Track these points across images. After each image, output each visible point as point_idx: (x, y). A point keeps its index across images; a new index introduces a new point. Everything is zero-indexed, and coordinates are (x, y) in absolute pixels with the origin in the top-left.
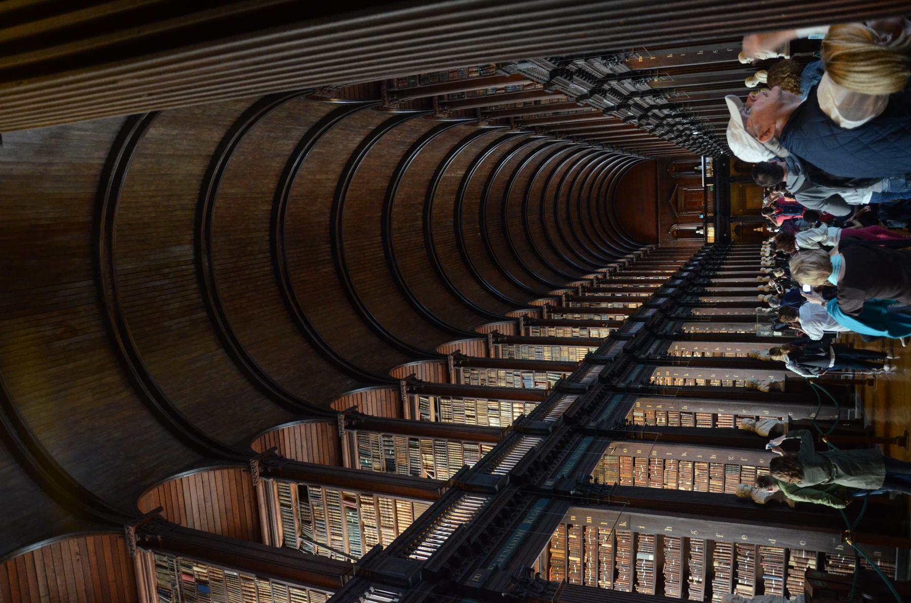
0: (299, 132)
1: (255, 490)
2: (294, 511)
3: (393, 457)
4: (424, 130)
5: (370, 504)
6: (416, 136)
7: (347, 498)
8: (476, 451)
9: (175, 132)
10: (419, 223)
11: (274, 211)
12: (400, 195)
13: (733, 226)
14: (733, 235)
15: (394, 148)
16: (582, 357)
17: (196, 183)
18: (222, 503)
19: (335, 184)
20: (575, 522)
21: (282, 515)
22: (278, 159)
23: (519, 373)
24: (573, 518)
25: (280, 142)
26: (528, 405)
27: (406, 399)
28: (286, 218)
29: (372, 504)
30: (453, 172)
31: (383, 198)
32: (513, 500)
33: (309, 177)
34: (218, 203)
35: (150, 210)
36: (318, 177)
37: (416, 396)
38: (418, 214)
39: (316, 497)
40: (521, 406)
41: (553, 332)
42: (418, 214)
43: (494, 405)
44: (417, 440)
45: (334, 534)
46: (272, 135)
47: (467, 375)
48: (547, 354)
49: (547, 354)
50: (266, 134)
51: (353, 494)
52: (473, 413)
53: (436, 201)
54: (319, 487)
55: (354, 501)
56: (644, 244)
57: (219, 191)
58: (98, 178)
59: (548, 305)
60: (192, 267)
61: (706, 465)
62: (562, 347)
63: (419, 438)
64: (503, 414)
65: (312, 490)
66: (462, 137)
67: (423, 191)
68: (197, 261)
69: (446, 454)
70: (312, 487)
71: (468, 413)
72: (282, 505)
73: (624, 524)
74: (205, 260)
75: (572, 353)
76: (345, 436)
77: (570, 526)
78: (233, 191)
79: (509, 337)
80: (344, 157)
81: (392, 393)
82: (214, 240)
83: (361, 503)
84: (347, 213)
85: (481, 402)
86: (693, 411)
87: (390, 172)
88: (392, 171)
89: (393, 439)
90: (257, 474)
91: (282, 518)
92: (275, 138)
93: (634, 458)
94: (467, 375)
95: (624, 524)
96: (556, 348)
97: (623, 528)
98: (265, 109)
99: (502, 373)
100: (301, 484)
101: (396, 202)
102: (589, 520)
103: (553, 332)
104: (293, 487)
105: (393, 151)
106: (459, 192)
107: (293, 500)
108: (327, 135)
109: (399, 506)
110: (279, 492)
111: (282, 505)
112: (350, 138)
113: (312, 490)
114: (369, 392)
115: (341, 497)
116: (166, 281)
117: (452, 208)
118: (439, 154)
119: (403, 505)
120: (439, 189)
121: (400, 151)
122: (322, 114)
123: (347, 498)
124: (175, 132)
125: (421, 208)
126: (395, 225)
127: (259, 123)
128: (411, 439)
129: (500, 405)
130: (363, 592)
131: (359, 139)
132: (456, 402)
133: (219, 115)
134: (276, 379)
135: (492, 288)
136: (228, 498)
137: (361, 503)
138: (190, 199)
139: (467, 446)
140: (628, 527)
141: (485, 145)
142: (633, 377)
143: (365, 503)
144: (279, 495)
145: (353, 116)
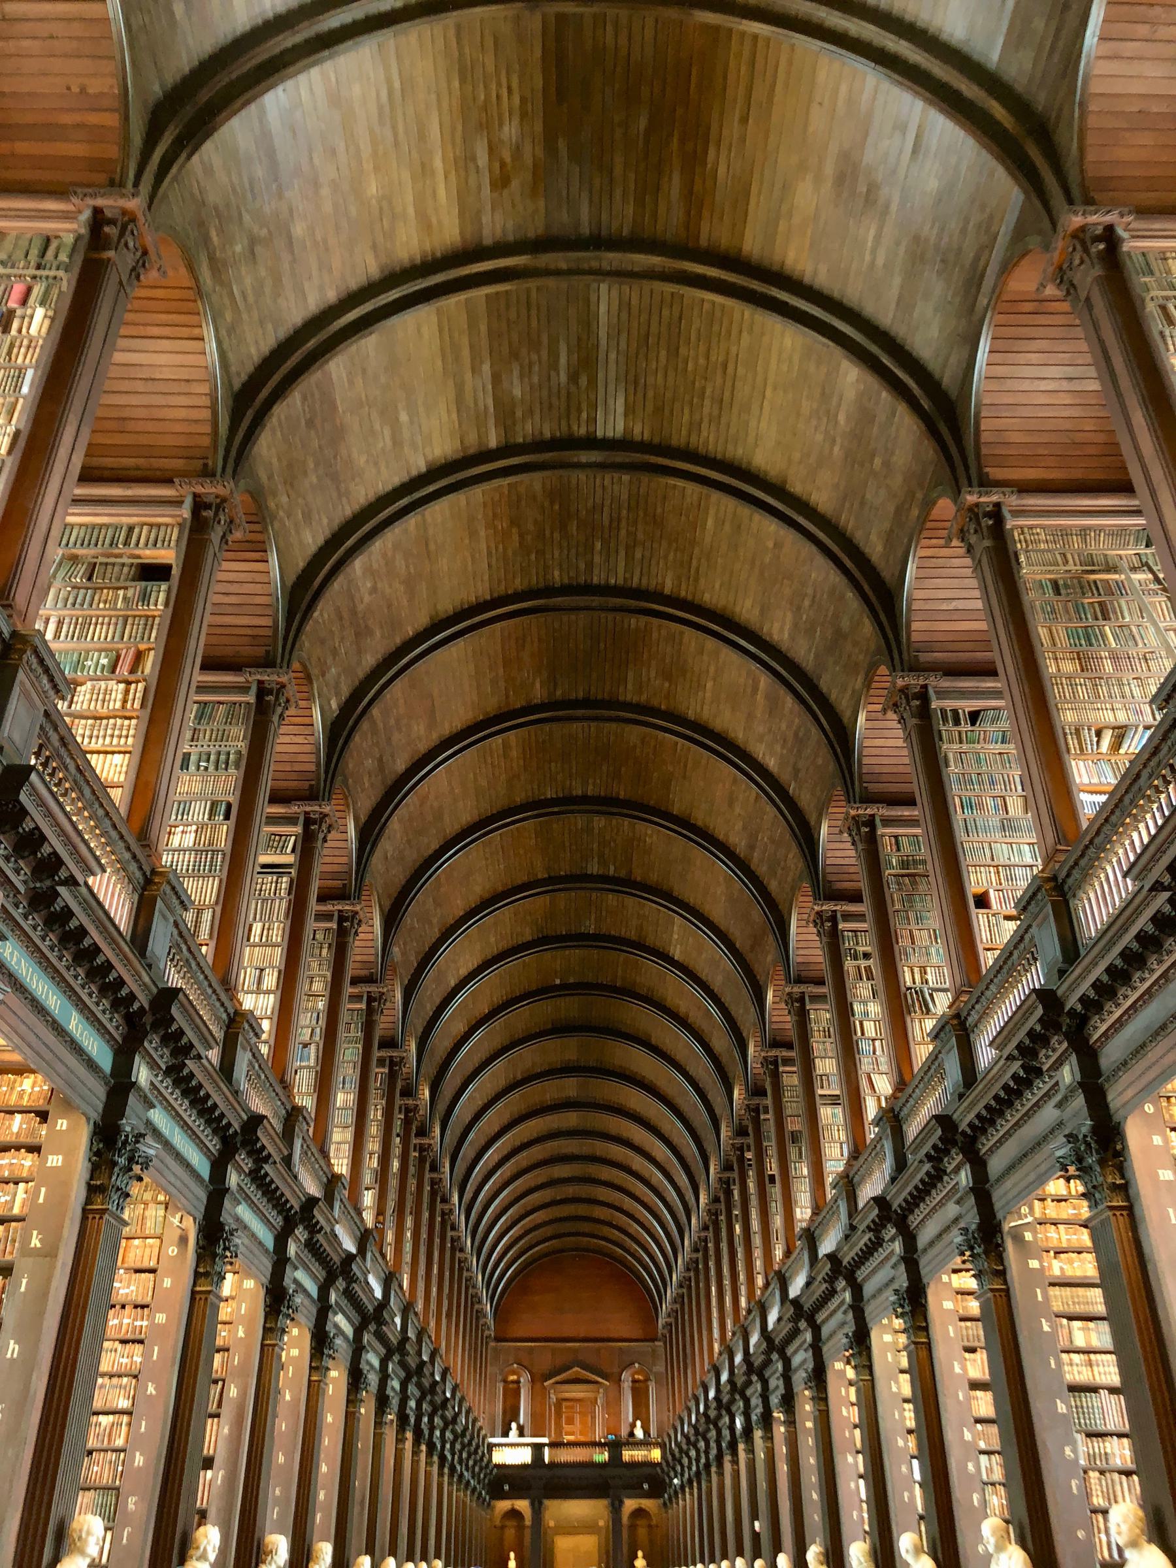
0: (803, 652)
1: (168, 481)
2: (116, 551)
3: (192, 768)
4: (773, 886)
5: (125, 701)
6: (762, 870)
7: (139, 657)
9: (842, 418)
10: (594, 868)
11: (658, 596)
12: (652, 835)
15: (744, 828)
16: (337, 1169)
17: (736, 452)
18: (142, 413)
19: (691, 715)
20: (52, 1130)
21: (107, 526)
22: (757, 612)
23: (318, 1038)
25: (789, 615)
27: (294, 809)
28: (643, 620)
29: (123, 707)
30: (681, 939)
31: (652, 803)
32: (124, 992)
33: (712, 669)
34: (692, 489)
35: (702, 361)
36: (709, 685)
37: (298, 829)
38: (612, 868)
39: (145, 597)
41: (375, 1114)
42: (612, 868)
43: (271, 980)
44: (227, 817)
45: (60, 623)
46: (807, 603)
47: (320, 936)
48: (344, 1098)
49: (344, 1098)
50: (810, 591)
51: (147, 670)
53: (630, 901)
54: (166, 604)
55: (132, 671)
57: (716, 496)
58: (775, 268)
60: (583, 431)
61: (120, 1442)
62: (351, 1130)
65: (160, 594)
66: (749, 957)
67: (654, 878)
68: (591, 442)
70: (169, 592)
72: (131, 529)
73: (35, 1242)
74: (594, 456)
75: (338, 1150)
76: (242, 679)
77: (43, 1116)
78: (710, 523)
80: (739, 734)
81: (306, 785)
82: (626, 478)
83: (128, 683)
84: (634, 733)
86: (226, 1411)
87: (700, 817)
88: (700, 823)
89: (232, 770)
90: (199, 489)
91: (101, 526)
92: (799, 608)
93: (153, 1271)
94: (320, 936)
95: (35, 1242)
96: (350, 1118)
97: (27, 1239)
98: (866, 587)
100: (176, 572)
101: (641, 826)
103: (375, 1114)
104: (167, 555)
105: (739, 826)
106: (640, 946)
107: (137, 552)
108: (789, 701)
109: (118, 758)
110: (159, 526)
111: (131, 529)
112: (778, 748)
113: (160, 594)
114: (311, 739)
115: (142, 647)
116: (563, 378)
117: (613, 933)
118: (717, 911)
120: (651, 908)
121: (737, 840)
122: (833, 697)
123: (139, 657)
124: (842, 418)
125: (623, 874)
126: (599, 822)
127: (835, 577)
128: (229, 806)
129: (268, 992)
131: (772, 763)
132: (281, 907)
133: (863, 503)
134: (358, 564)
135: (459, 999)
136: (150, 426)
137: (128, 683)
138: (709, 440)
139: (207, 916)
140: (26, 1251)
141: (727, 999)
142: (300, 1275)
143: (127, 692)
144: (151, 525)
145: (825, 751)
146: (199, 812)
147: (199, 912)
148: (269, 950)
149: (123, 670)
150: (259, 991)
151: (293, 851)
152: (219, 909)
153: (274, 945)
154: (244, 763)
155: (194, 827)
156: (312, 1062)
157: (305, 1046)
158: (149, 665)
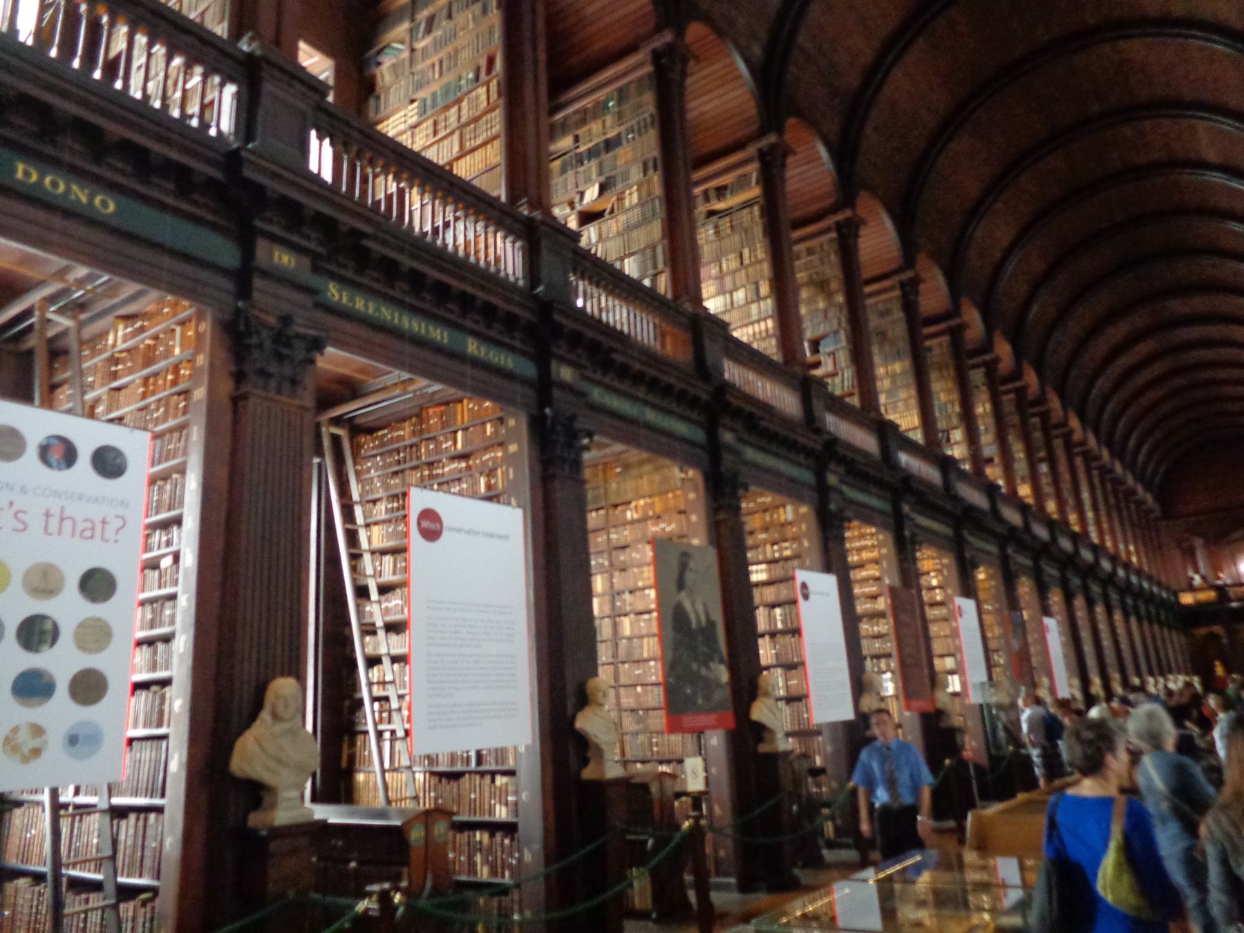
7: (491, 61)
8: (655, 267)
13: (1217, 629)
14: (1203, 631)
23: (844, 323)
24: (512, 422)
26: (774, 341)
40: (771, 332)
43: (765, 289)
47: (826, 247)
52: (746, 261)
56: (1157, 499)
59: (996, 361)
63: (659, 172)
64: (754, 307)
69: (644, 221)
71: (746, 252)
79: (916, 303)
85: (766, 268)
99: (840, 298)
102: (513, 448)
119: (495, 154)
129: (766, 298)
130: (215, 71)
137: (487, 84)
139: (659, 250)
146: (636, 174)
147: (654, 248)
148: (758, 266)
149: (483, 77)
150: (759, 299)
151: (757, 183)
152: (665, 242)
153: (760, 262)
154: (657, 123)
155: (635, 188)
156: (844, 343)
157: (836, 333)
158: (499, 65)
